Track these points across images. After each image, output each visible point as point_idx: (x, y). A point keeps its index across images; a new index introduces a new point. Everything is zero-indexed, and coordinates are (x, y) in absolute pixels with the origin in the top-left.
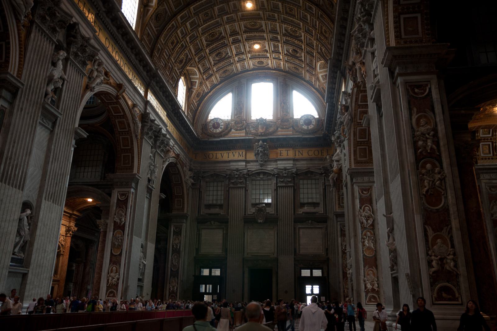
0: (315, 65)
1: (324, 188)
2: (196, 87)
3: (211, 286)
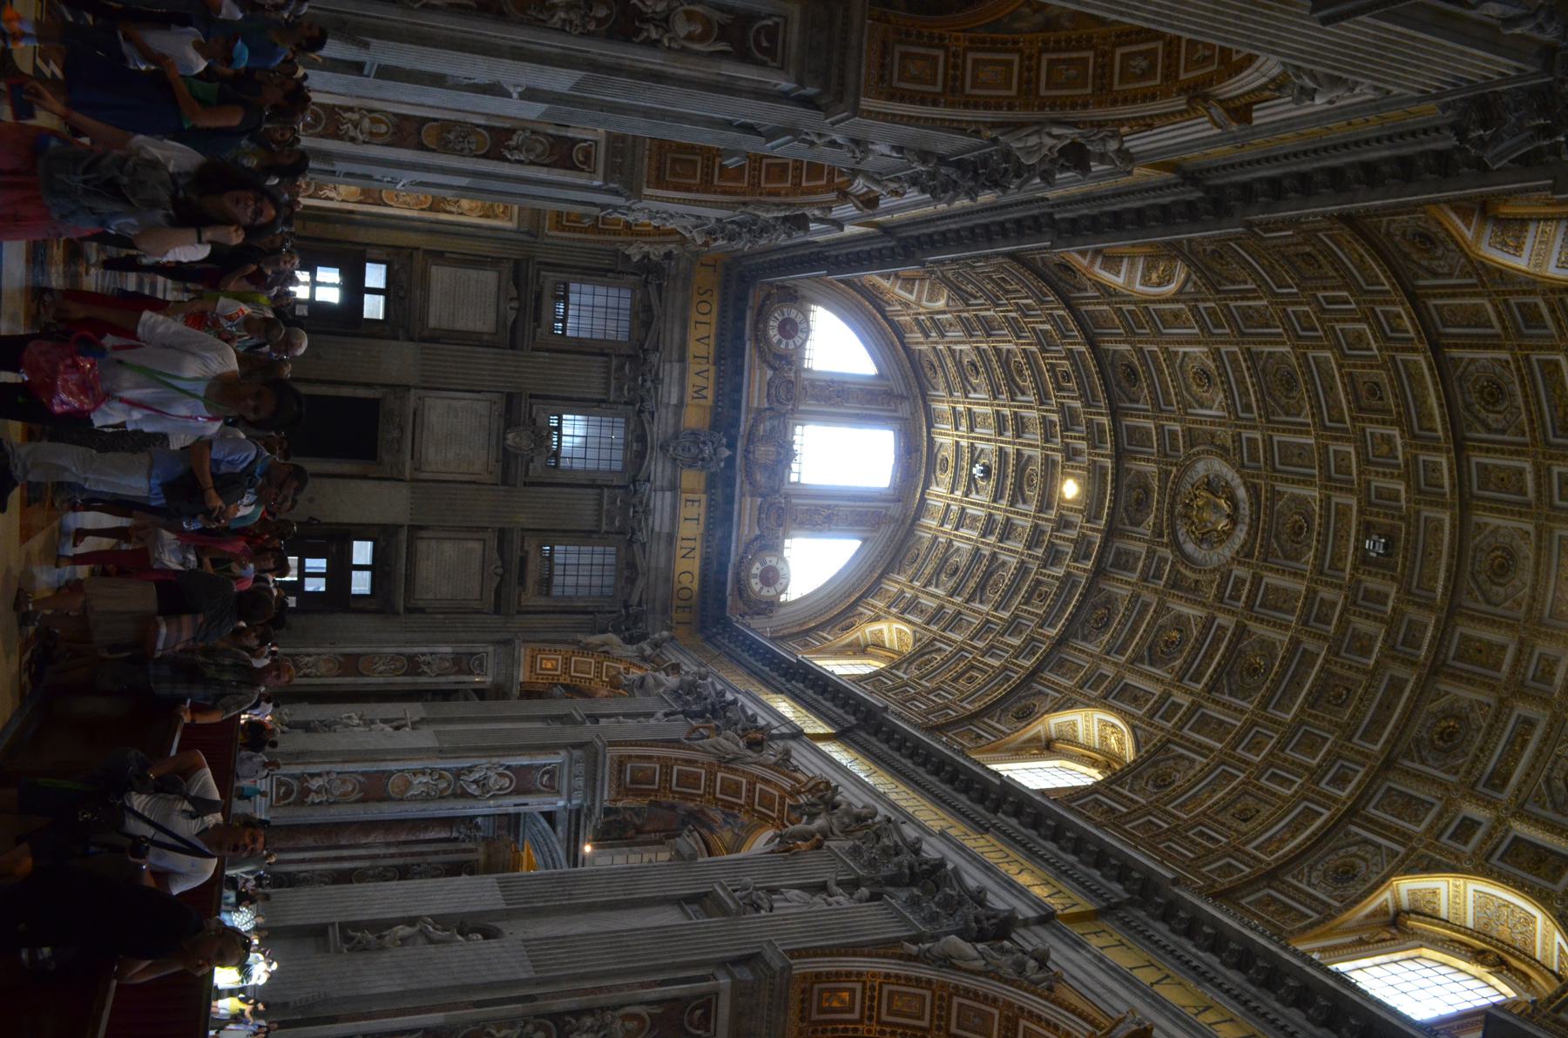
0: (909, 622)
2: (897, 290)
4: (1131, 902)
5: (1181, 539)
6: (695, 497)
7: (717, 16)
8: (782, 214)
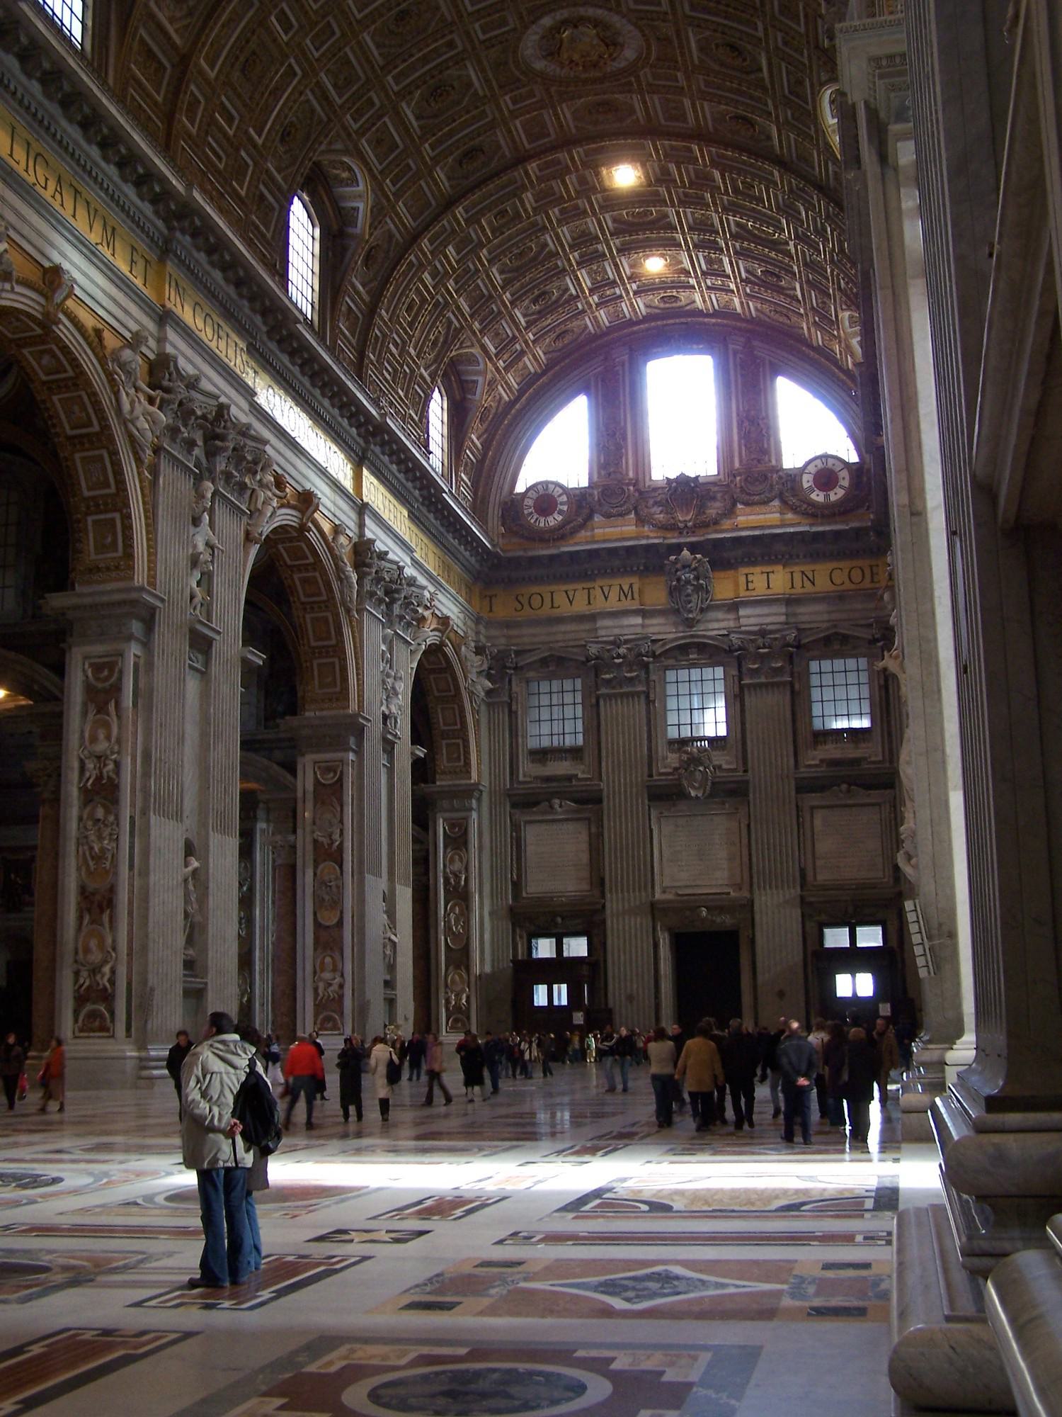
0: (837, 316)
1: (882, 682)
3: (564, 987)
5: (623, 64)
7: (91, 716)
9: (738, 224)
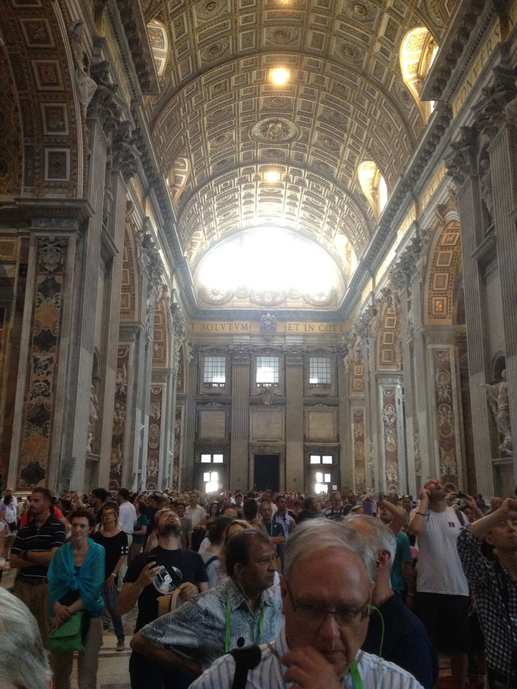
4: (412, 190)
5: (287, 138)
6: (288, 326)
8: (171, 315)
9: (307, 199)
